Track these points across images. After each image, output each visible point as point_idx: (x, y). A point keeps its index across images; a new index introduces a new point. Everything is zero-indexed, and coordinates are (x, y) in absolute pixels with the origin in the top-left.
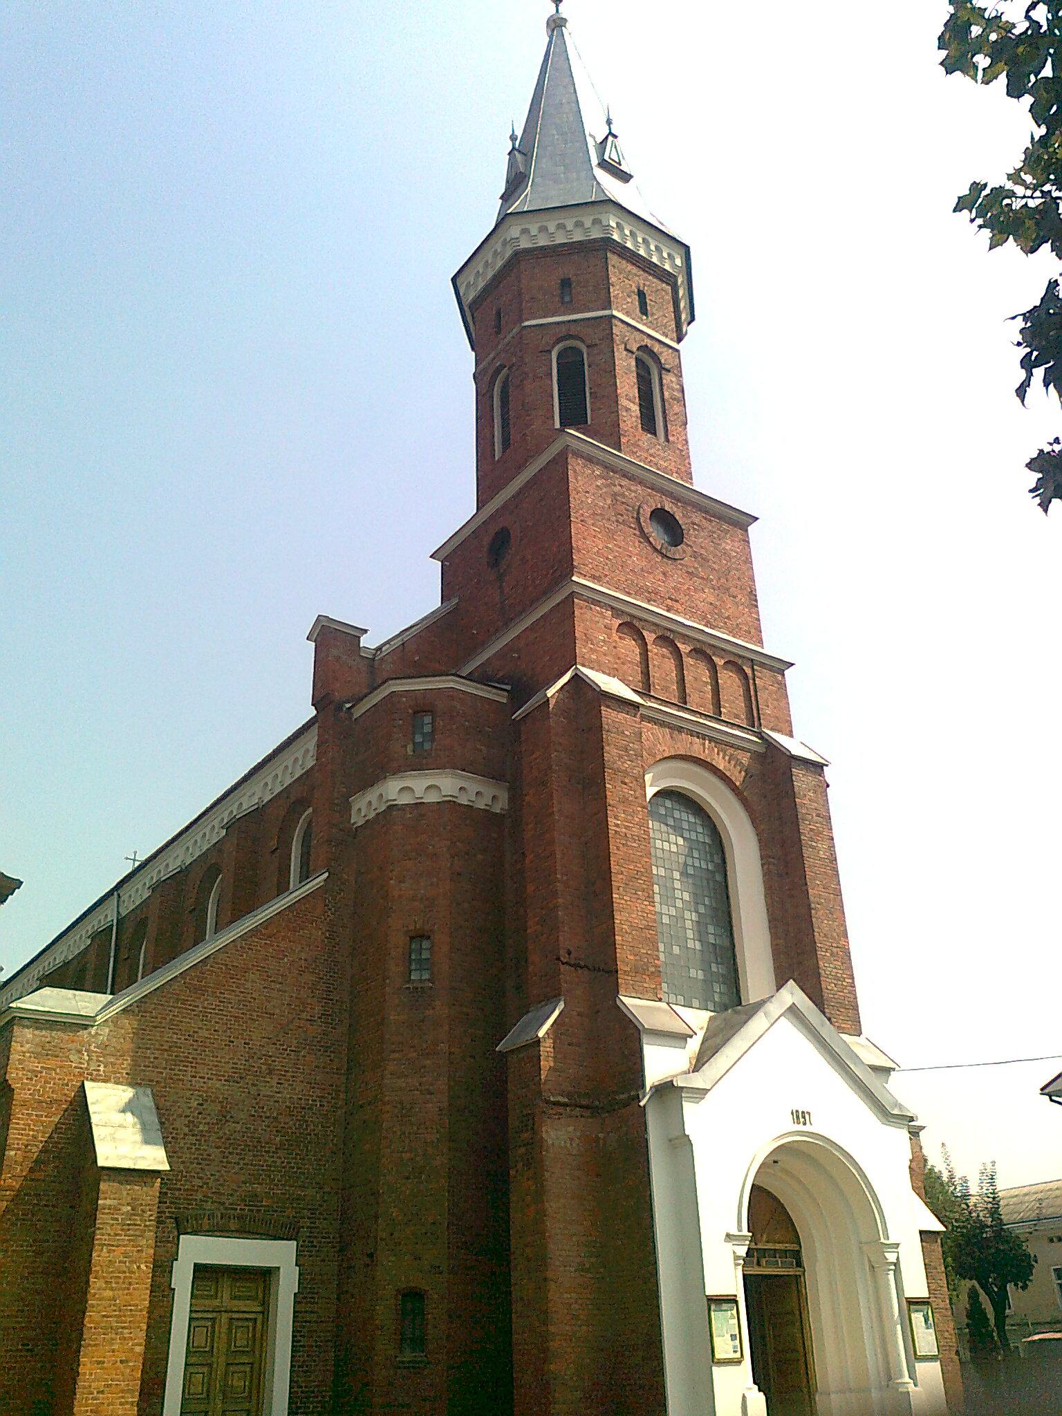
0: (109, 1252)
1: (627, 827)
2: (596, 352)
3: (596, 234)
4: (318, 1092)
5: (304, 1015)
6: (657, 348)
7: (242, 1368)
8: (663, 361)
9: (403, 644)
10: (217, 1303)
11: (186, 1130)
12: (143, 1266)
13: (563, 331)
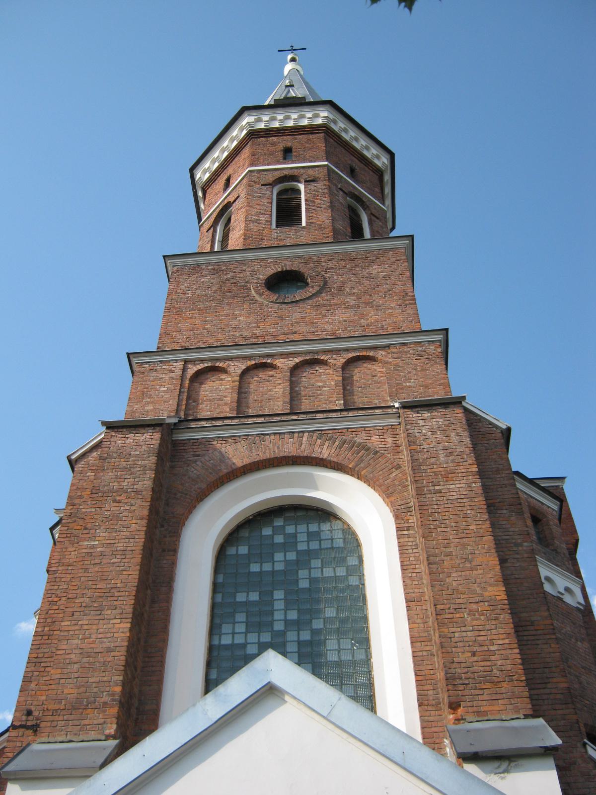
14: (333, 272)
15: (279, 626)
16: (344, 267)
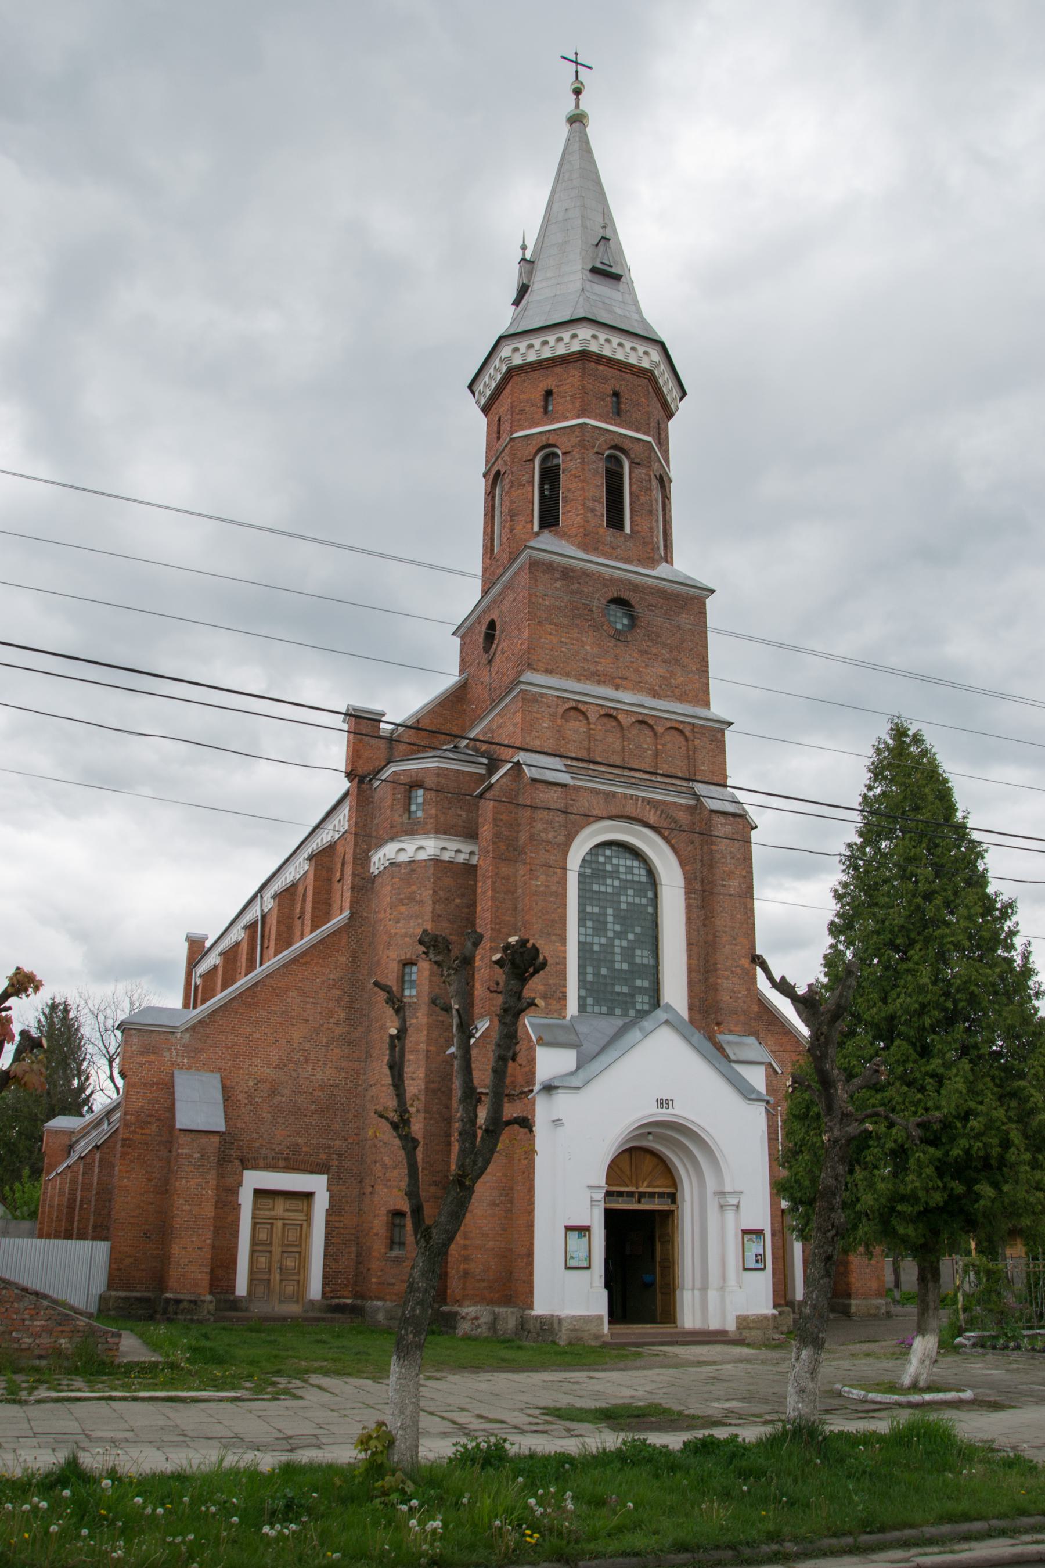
0: (187, 1182)
1: (547, 886)
2: (568, 459)
3: (576, 347)
4: (343, 1075)
5: (332, 1020)
6: (627, 445)
7: (293, 1255)
8: (633, 456)
10: (273, 1213)
11: (246, 1101)
12: (209, 1192)
13: (543, 440)
14: (653, 611)
15: (610, 934)
16: (662, 608)
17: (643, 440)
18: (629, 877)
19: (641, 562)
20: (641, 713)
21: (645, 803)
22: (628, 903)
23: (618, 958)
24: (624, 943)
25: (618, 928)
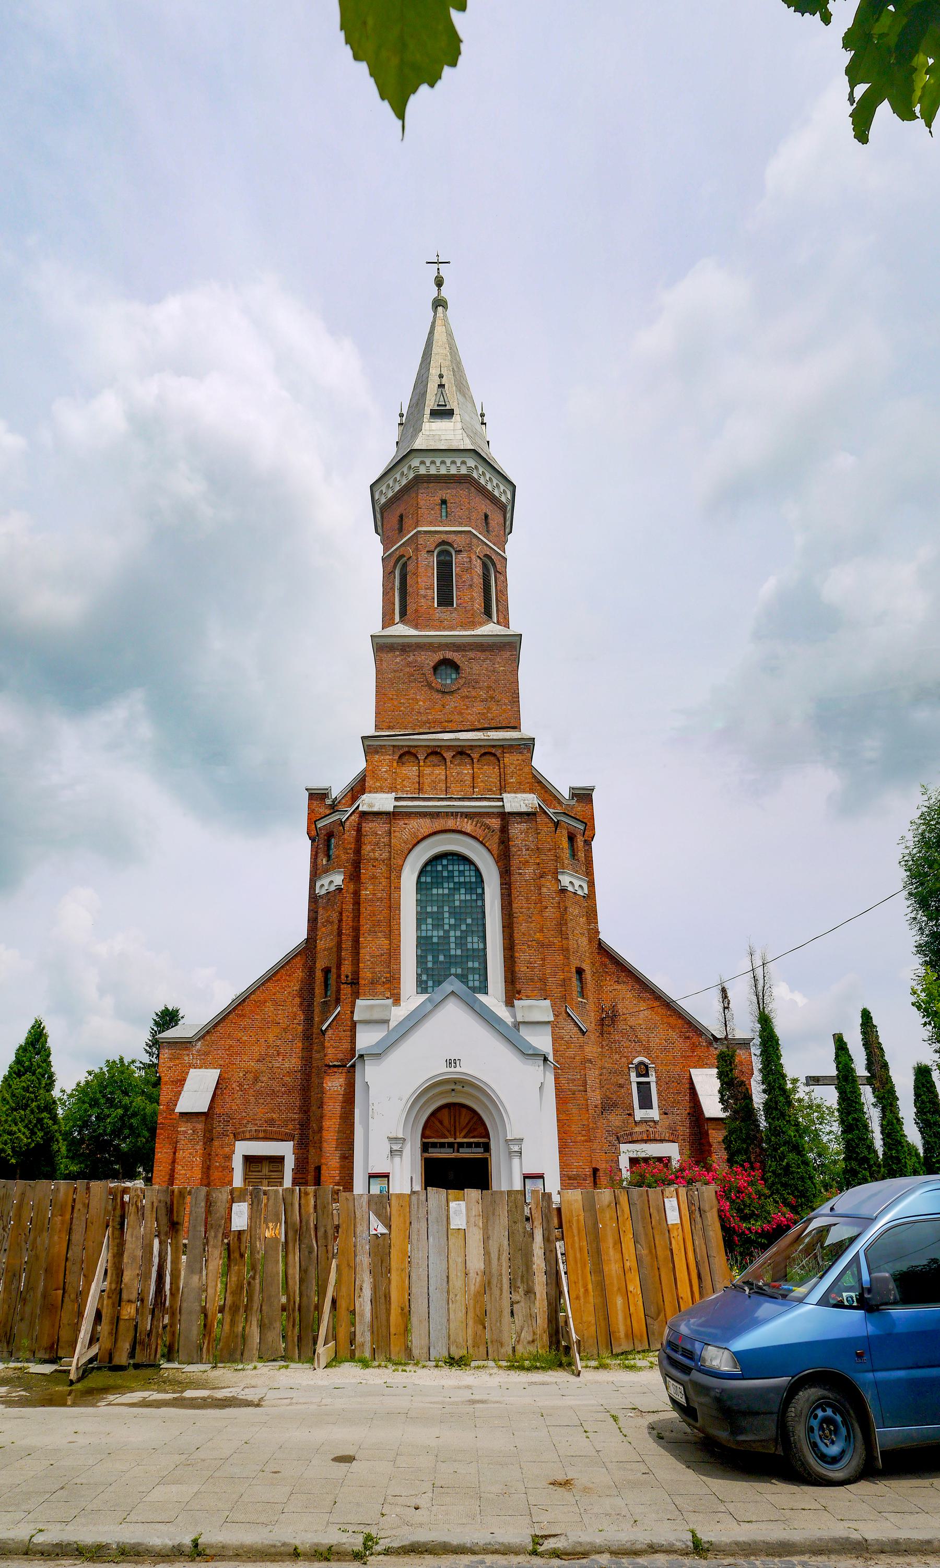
5: (295, 1021)
6: (451, 538)
8: (455, 546)
9: (352, 788)
15: (447, 927)
17: (464, 531)
18: (462, 879)
19: (464, 626)
20: (460, 746)
21: (464, 817)
22: (460, 901)
23: (453, 946)
24: (458, 934)
25: (452, 921)
